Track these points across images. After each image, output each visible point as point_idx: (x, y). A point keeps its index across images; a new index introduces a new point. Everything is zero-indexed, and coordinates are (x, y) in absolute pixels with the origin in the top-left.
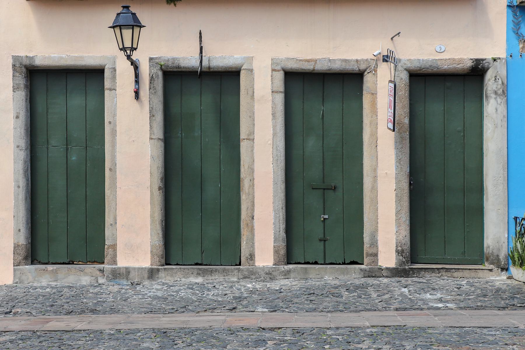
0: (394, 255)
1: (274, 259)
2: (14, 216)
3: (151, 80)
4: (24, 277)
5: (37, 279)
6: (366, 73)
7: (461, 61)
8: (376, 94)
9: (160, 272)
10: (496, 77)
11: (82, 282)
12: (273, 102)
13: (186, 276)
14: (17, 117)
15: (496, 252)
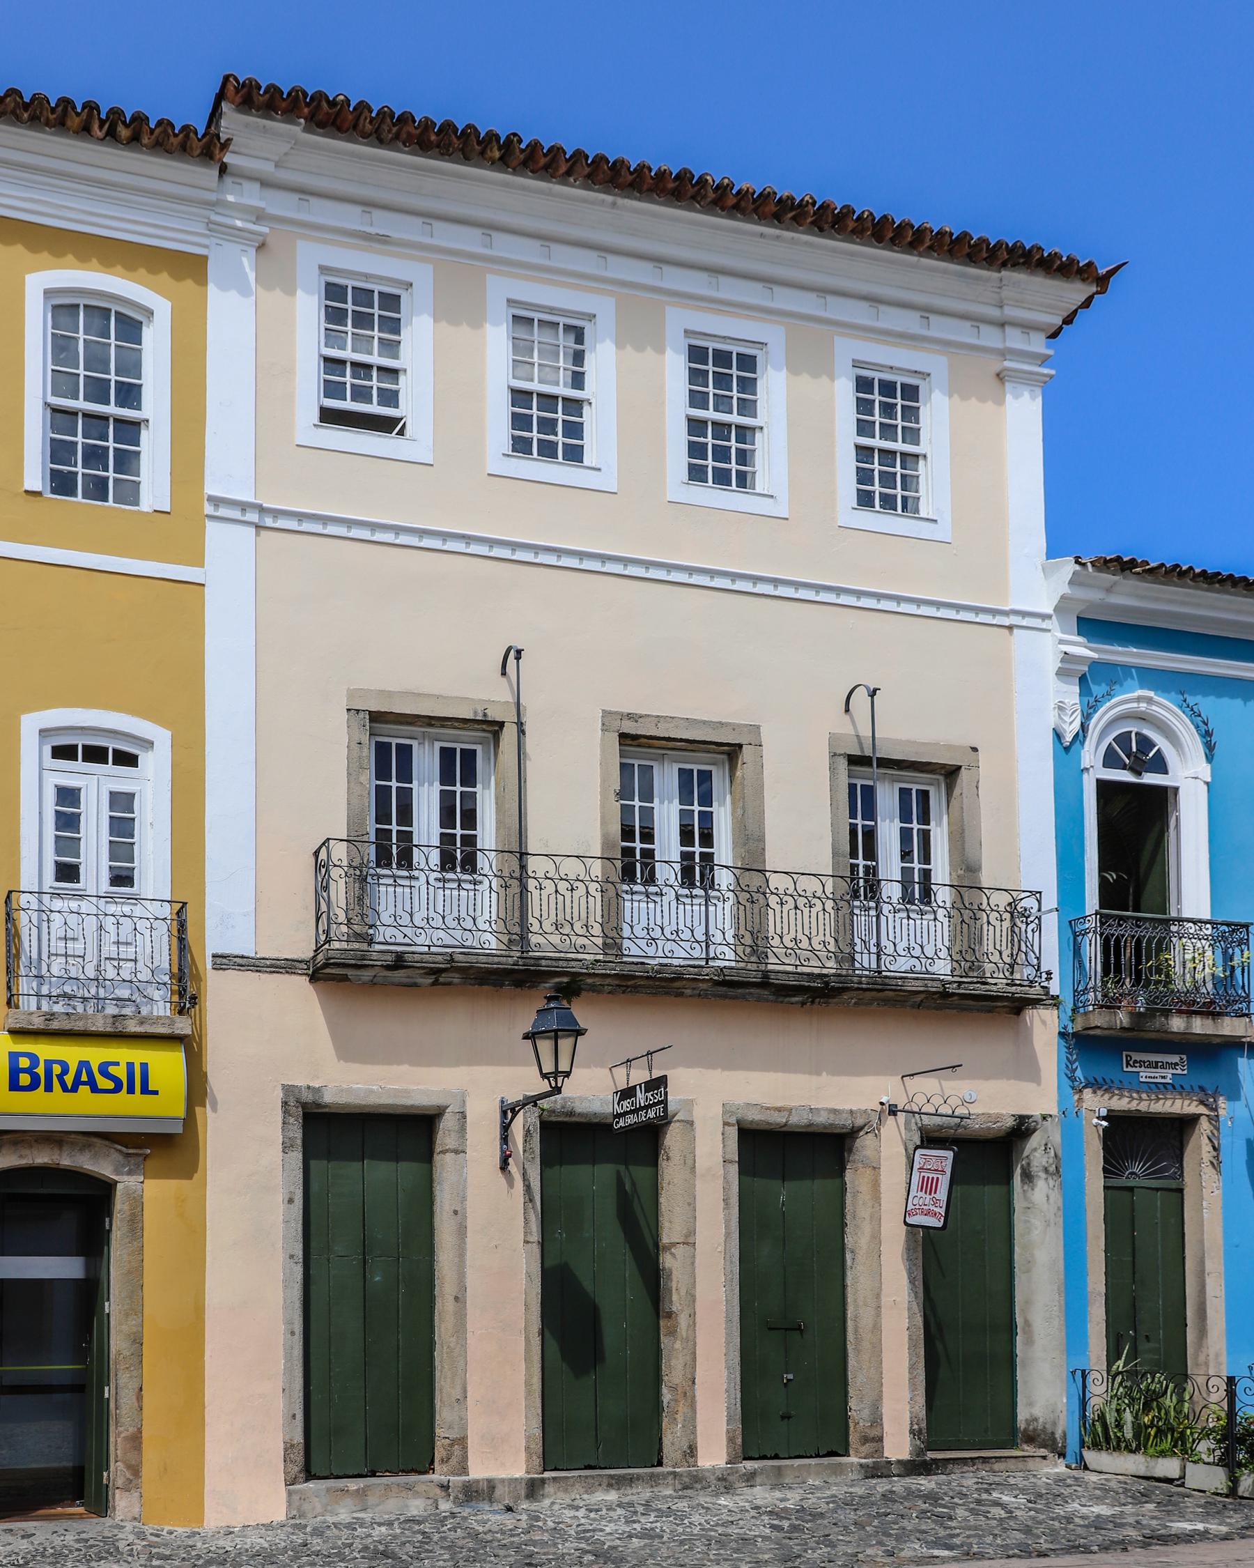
0: (907, 1438)
1: (728, 1454)
2: (284, 1390)
3: (526, 1136)
4: (306, 1507)
5: (329, 1508)
6: (861, 1133)
7: (997, 1119)
8: (880, 1168)
9: (546, 1485)
10: (1046, 1144)
11: (412, 1509)
12: (725, 1178)
13: (590, 1490)
14: (291, 1201)
15: (1049, 1428)
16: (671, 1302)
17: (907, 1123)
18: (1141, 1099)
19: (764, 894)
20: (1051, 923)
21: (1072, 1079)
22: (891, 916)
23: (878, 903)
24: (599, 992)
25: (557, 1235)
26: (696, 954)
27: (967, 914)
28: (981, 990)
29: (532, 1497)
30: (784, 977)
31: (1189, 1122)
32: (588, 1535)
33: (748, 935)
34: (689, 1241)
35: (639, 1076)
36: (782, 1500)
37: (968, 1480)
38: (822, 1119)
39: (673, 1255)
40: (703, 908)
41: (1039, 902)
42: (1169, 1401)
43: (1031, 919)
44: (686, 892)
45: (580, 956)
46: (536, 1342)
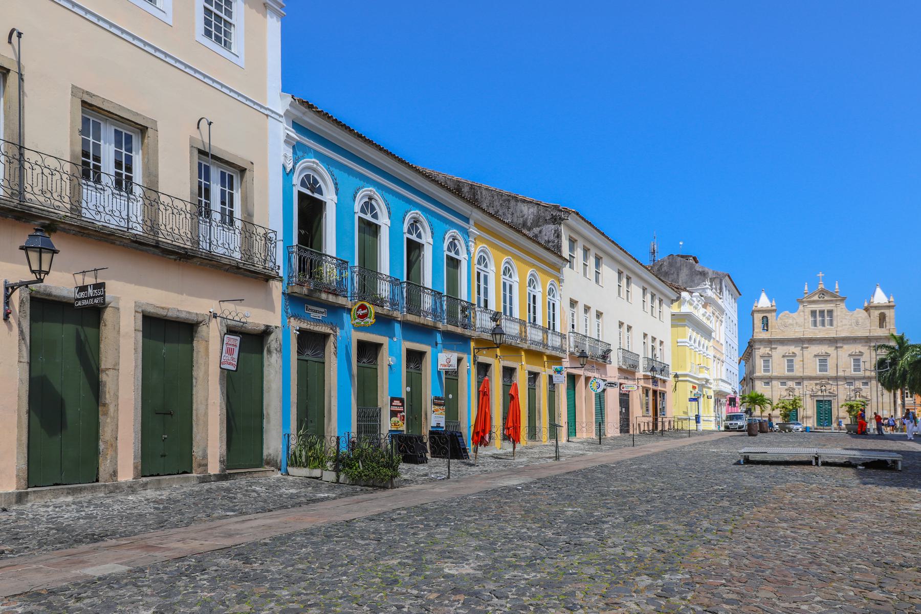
0: (218, 464)
1: (134, 474)
13: (56, 497)
16: (105, 398)
17: (221, 322)
18: (311, 325)
19: (157, 203)
20: (280, 245)
21: (287, 312)
22: (216, 228)
23: (210, 220)
24: (68, 233)
25: (40, 360)
26: (122, 224)
27: (248, 234)
28: (252, 268)
29: (20, 502)
30: (167, 245)
31: (326, 336)
32: (54, 520)
33: (149, 221)
34: (116, 368)
35: (90, 280)
36: (160, 495)
37: (242, 482)
38: (183, 315)
39: (107, 374)
40: (126, 203)
41: (276, 235)
42: (318, 446)
43: (273, 242)
44: (117, 192)
45: (56, 211)
46: (25, 417)
